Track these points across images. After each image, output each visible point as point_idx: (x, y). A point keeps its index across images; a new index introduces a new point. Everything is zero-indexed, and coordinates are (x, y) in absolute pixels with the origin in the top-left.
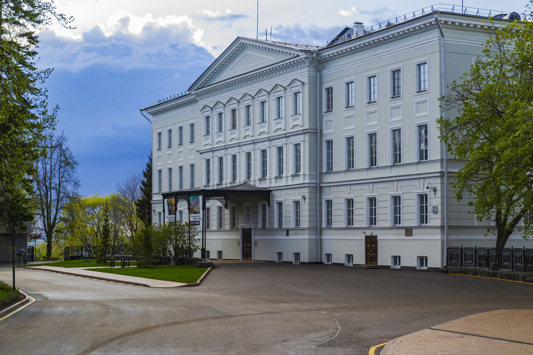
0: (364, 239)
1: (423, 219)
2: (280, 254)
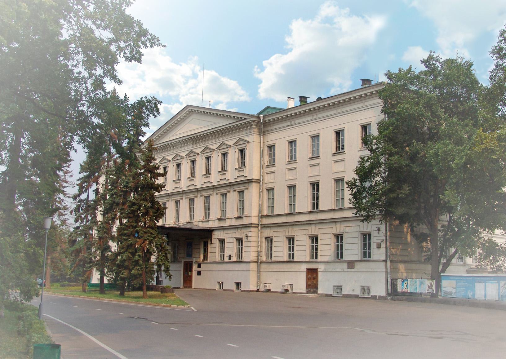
0: (305, 271)
1: (366, 254)
2: (221, 284)
